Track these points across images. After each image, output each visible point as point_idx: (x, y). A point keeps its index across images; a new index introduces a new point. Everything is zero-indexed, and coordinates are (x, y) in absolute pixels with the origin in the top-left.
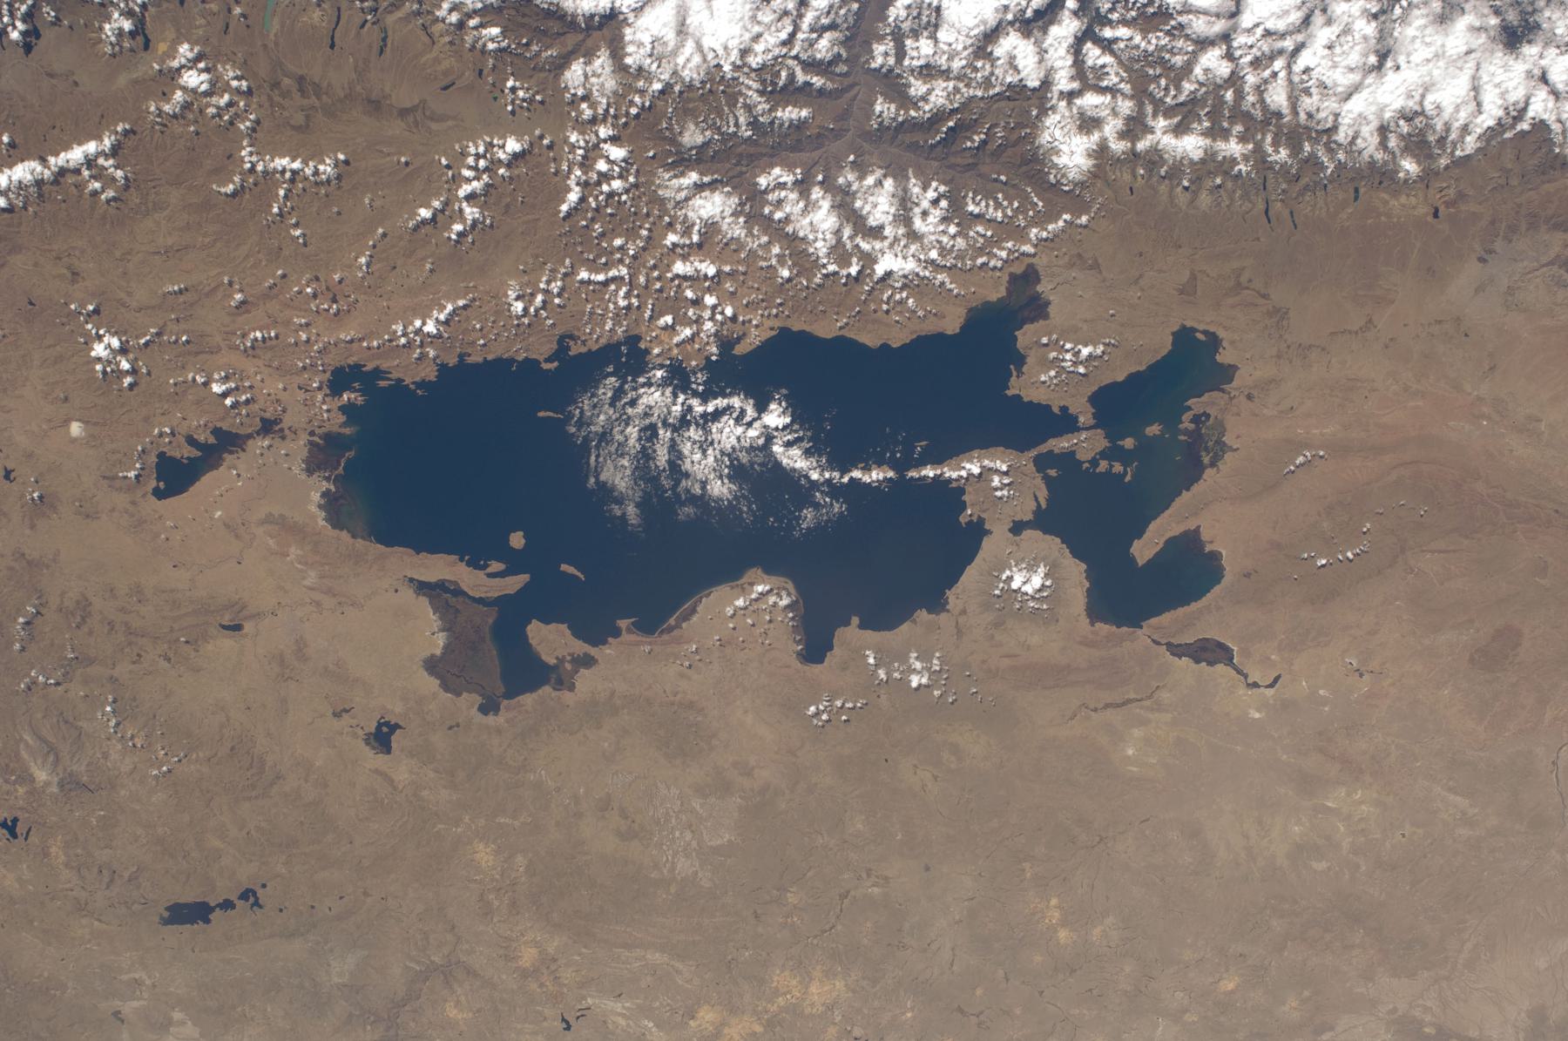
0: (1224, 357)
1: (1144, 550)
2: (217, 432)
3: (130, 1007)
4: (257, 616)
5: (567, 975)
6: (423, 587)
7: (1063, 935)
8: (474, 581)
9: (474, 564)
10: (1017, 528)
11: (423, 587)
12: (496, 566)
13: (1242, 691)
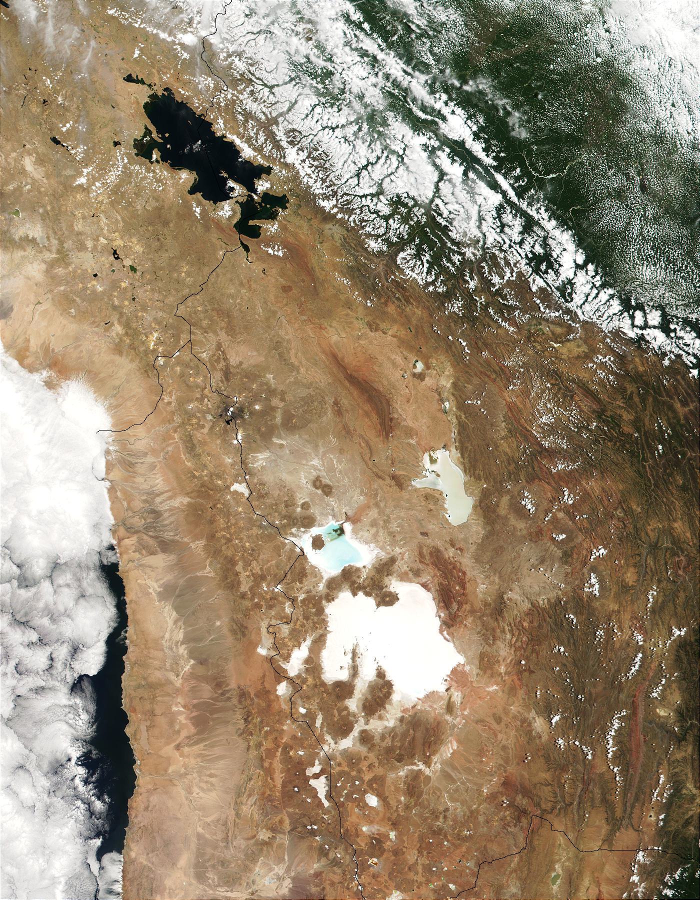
0: (287, 205)
1: (251, 223)
2: (142, 79)
3: (28, 146)
4: (119, 109)
5: (103, 207)
6: (146, 128)
7: (183, 274)
8: (154, 135)
9: (157, 132)
10: (237, 202)
11: (146, 128)
12: (160, 136)
13: (245, 259)
